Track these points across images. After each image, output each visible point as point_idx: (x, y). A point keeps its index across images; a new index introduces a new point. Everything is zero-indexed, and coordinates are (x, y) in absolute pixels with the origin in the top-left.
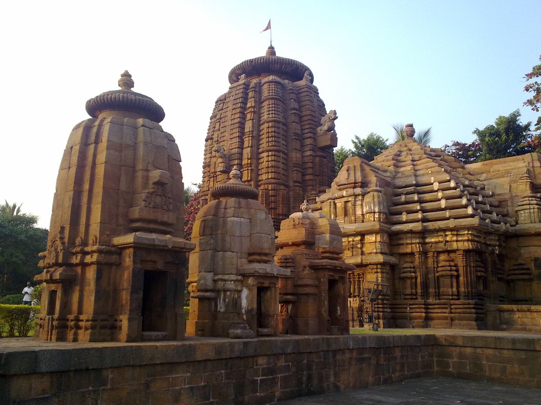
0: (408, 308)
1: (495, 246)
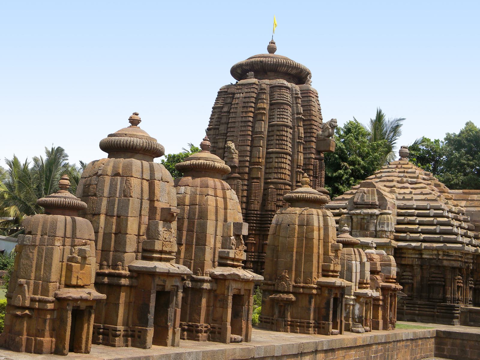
0: (405, 307)
1: (470, 263)
